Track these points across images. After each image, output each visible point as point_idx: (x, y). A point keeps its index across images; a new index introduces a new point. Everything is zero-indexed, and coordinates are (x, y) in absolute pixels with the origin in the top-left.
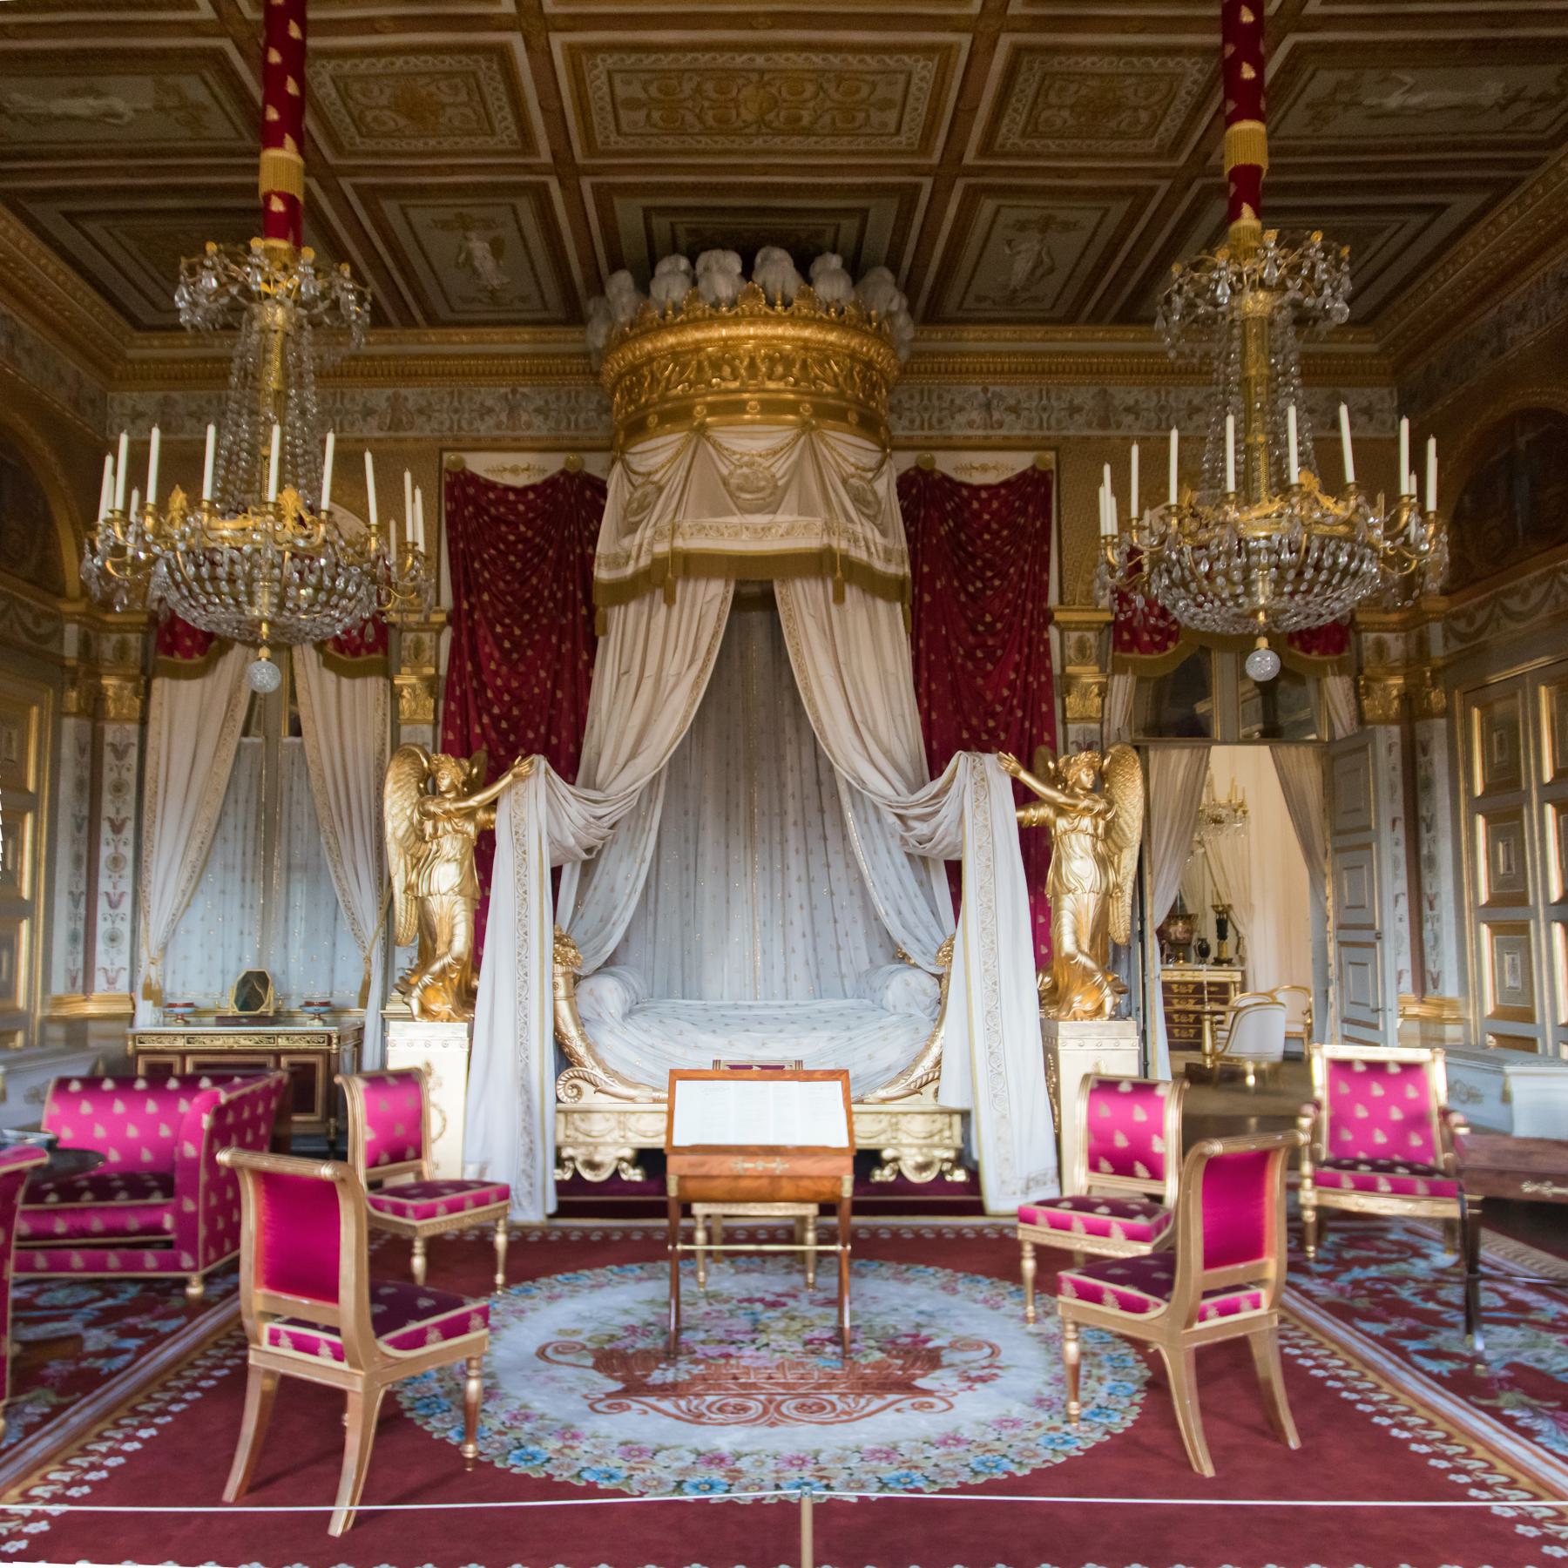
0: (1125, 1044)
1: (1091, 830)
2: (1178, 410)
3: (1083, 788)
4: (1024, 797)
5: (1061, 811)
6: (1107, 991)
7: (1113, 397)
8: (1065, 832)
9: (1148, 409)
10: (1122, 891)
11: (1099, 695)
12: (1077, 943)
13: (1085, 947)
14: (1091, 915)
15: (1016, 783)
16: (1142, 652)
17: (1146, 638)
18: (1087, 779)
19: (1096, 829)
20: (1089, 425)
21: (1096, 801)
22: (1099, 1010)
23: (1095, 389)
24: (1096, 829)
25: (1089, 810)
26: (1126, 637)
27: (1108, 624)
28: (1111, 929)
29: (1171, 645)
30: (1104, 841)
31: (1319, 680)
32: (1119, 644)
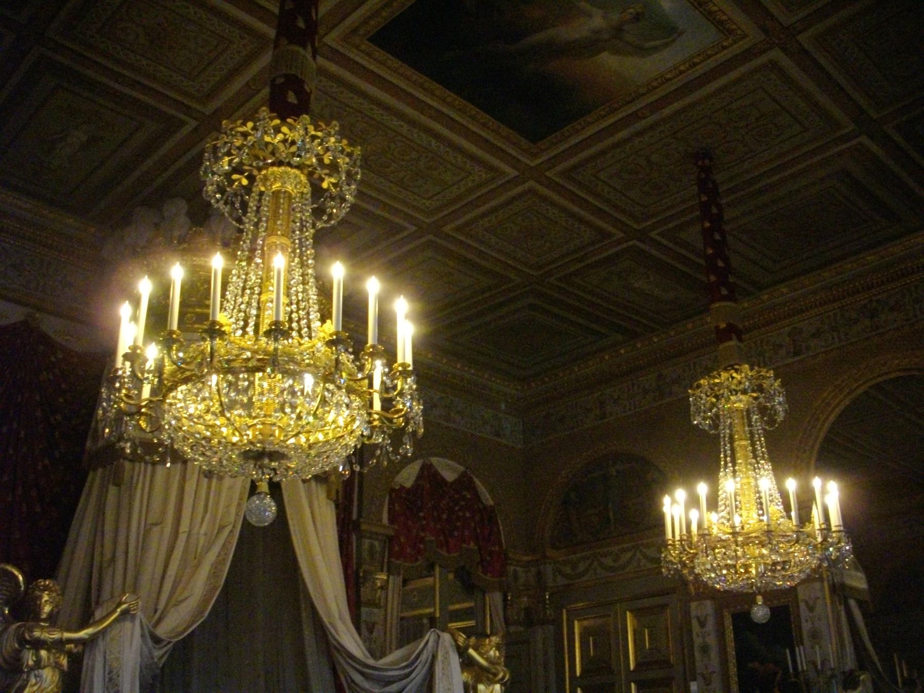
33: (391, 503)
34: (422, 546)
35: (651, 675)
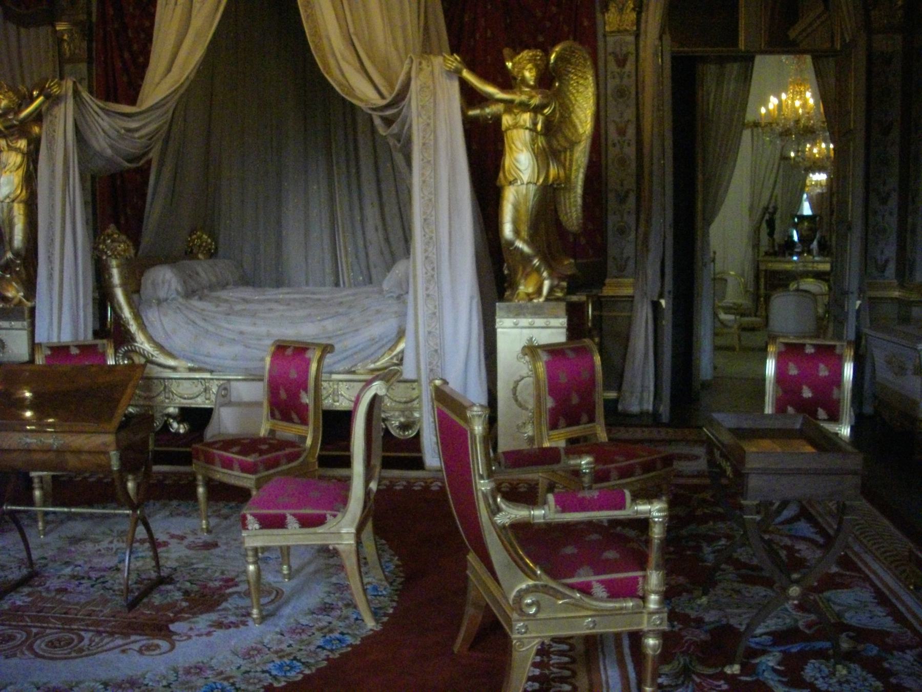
0: (555, 322)
3: (528, 86)
4: (470, 96)
5: (509, 106)
6: (545, 274)
8: (508, 129)
11: (634, 9)
12: (517, 232)
13: (524, 234)
14: (530, 204)
15: (464, 84)
19: (535, 124)
24: (535, 124)
28: (563, 218)
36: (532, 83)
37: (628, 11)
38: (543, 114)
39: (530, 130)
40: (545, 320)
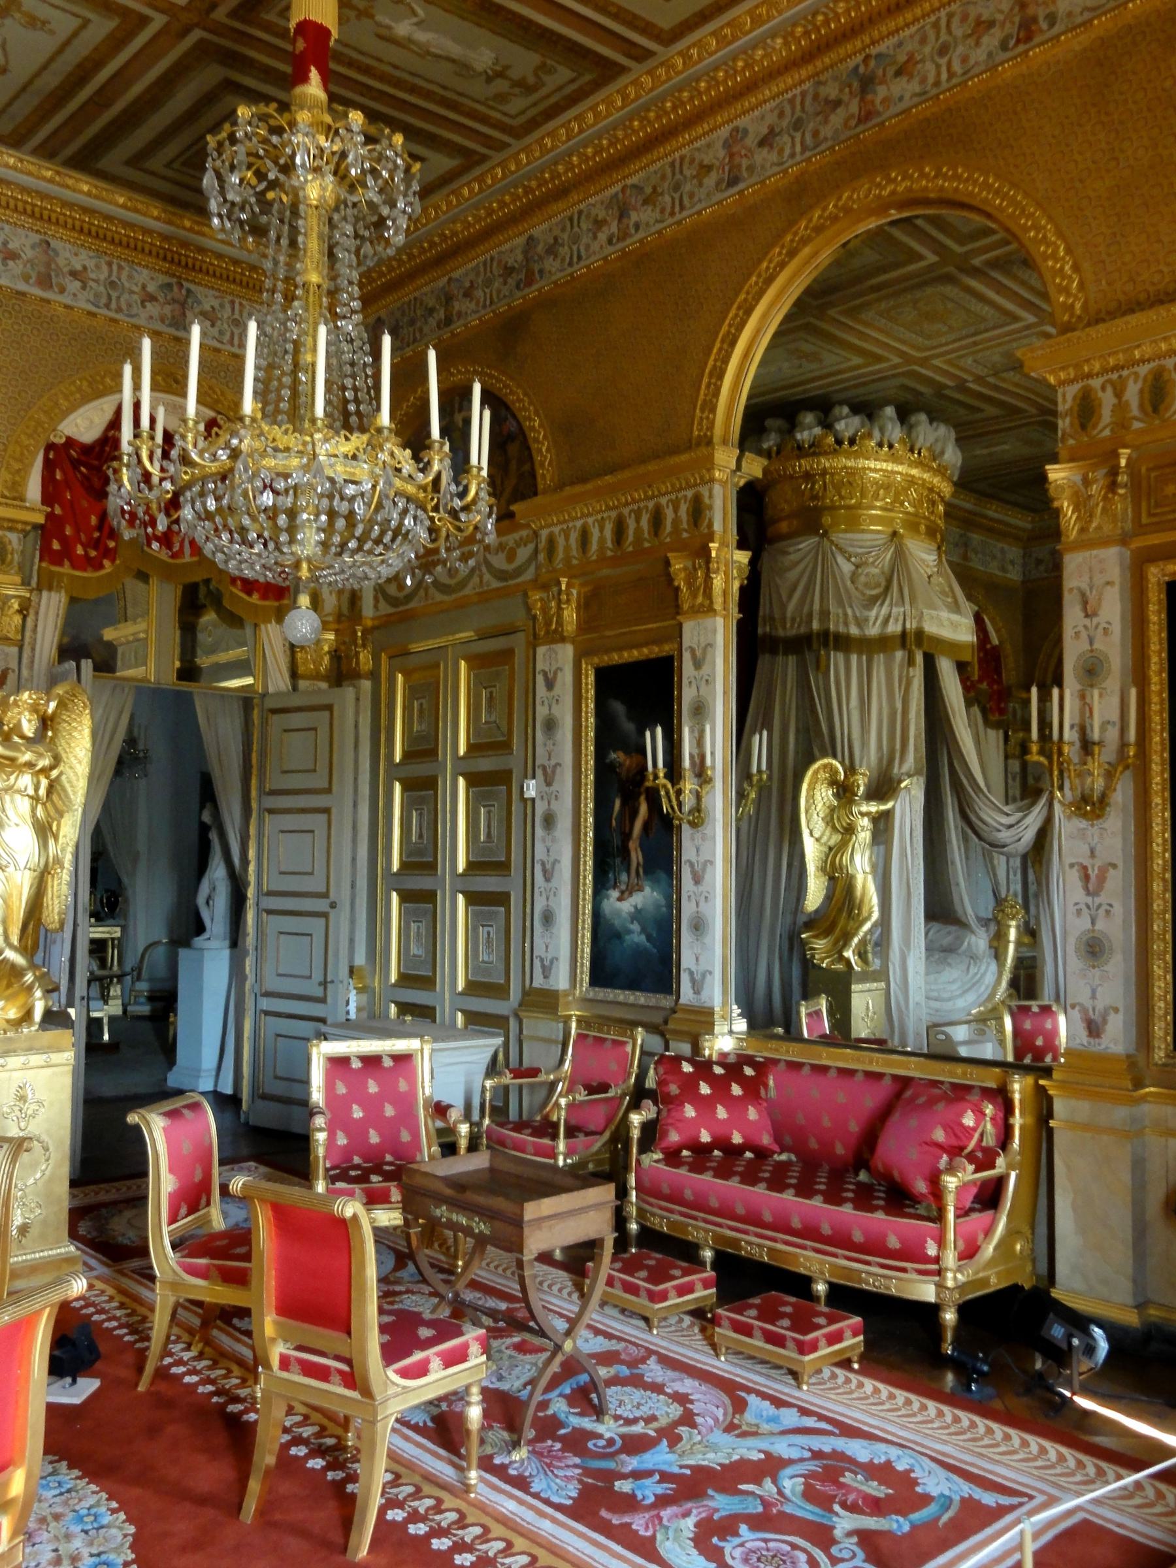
0: (56, 1058)
1: (31, 792)
2: (132, 292)
3: (23, 737)
6: (38, 993)
7: (57, 254)
9: (96, 281)
10: (62, 868)
11: (20, 611)
13: (15, 940)
16: (74, 566)
17: (80, 551)
18: (29, 727)
19: (37, 789)
20: (26, 278)
21: (41, 755)
22: (27, 1016)
23: (36, 238)
24: (37, 789)
25: (30, 765)
26: (56, 545)
27: (36, 527)
29: (106, 563)
30: (44, 804)
31: (256, 625)
32: (46, 553)
33: (49, 466)
34: (112, 544)
35: (486, 764)
36: (31, 735)
37: (12, 611)
38: (47, 777)
39: (31, 797)
40: (44, 1056)
